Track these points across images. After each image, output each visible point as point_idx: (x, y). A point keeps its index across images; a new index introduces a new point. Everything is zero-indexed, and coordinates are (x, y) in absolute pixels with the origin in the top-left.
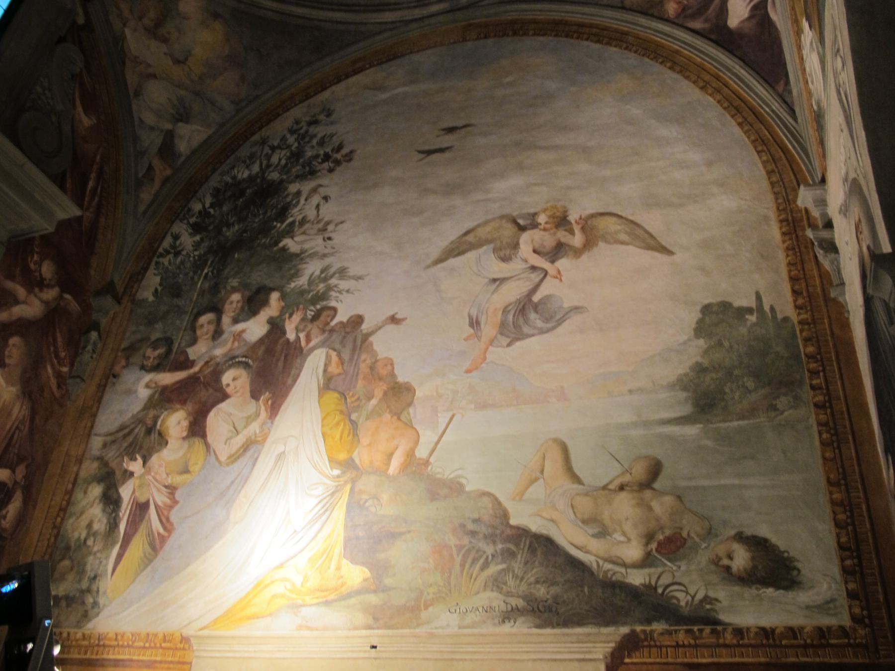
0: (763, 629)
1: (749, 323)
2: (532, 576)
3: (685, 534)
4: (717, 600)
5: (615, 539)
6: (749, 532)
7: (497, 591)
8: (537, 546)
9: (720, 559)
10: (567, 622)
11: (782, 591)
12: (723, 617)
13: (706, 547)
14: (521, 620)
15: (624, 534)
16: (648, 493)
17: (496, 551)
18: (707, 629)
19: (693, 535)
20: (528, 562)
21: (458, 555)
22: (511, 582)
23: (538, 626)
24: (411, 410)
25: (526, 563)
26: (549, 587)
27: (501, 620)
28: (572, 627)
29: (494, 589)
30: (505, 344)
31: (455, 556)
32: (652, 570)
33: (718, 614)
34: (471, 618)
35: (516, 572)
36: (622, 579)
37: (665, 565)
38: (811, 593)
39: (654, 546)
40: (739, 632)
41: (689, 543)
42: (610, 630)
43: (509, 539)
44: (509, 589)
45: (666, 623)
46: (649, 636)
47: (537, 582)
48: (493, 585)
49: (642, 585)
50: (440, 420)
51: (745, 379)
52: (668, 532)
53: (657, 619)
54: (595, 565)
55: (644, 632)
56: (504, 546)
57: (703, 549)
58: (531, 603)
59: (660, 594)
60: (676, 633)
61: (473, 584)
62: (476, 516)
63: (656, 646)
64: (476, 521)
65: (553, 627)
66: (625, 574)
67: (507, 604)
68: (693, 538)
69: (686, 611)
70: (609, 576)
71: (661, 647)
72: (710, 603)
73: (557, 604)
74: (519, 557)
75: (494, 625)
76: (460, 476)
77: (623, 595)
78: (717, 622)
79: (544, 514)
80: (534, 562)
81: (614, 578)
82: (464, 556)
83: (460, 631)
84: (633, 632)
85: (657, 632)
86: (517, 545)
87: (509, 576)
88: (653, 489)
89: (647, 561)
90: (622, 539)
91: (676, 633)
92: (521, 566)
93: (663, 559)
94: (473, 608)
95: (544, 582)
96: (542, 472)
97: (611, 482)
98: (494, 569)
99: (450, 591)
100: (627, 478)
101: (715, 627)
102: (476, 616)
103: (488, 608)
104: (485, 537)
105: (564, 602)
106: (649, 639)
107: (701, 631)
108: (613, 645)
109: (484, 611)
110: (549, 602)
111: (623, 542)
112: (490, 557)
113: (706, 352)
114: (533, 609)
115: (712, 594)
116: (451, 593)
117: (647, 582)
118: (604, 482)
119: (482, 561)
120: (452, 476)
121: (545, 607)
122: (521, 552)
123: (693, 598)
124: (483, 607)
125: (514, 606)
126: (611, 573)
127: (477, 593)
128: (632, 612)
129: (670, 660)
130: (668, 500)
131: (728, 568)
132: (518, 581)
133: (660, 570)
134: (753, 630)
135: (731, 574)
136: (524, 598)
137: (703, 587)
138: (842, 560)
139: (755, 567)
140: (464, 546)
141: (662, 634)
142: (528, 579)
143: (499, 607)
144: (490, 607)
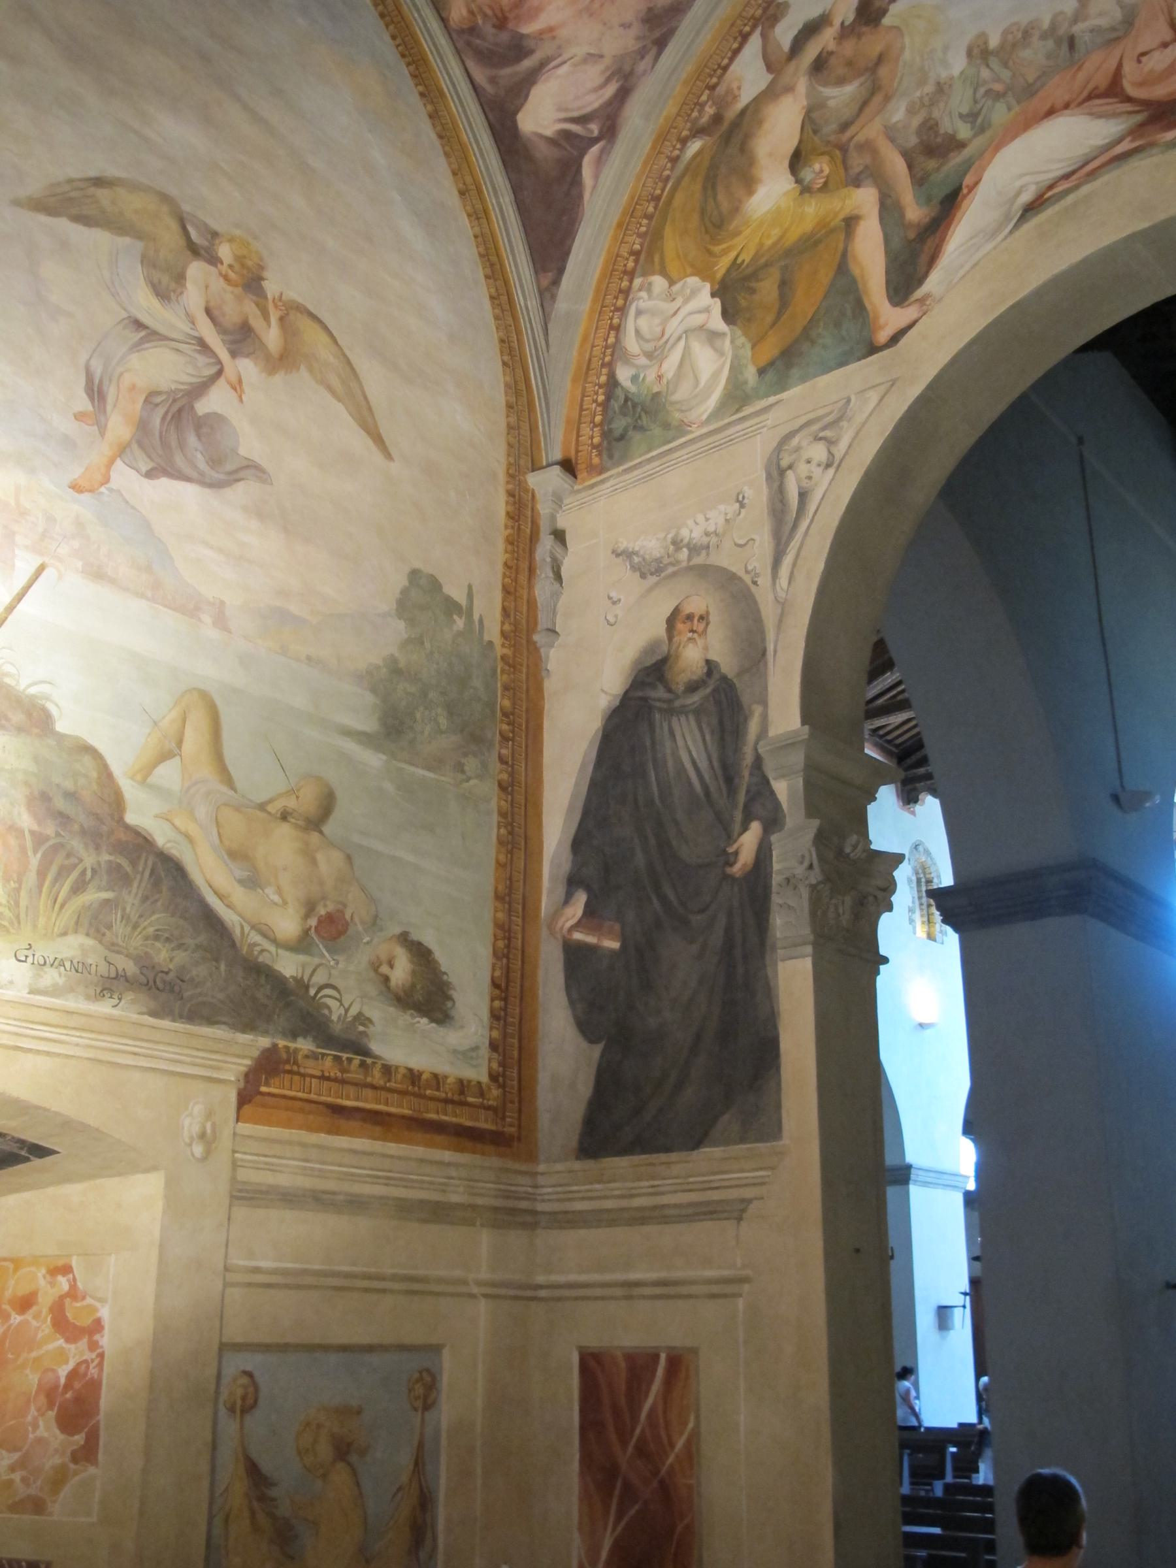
0: (410, 1070)
1: (455, 628)
2: (150, 925)
3: (348, 917)
5: (267, 896)
6: (415, 936)
7: (95, 938)
9: (381, 964)
10: (192, 1016)
11: (434, 1025)
12: (375, 1047)
13: (368, 943)
14: (129, 996)
15: (279, 892)
16: (314, 837)
17: (99, 863)
18: (357, 1059)
19: (356, 919)
21: (35, 852)
22: (120, 928)
23: (154, 1014)
25: (145, 899)
26: (173, 950)
27: (98, 992)
28: (200, 1025)
31: (30, 853)
33: (369, 1041)
34: (52, 976)
35: (128, 910)
36: (269, 962)
37: (323, 956)
39: (313, 922)
40: (387, 1070)
41: (351, 931)
43: (119, 848)
45: (314, 1041)
46: (292, 1055)
47: (157, 938)
48: (90, 924)
49: (292, 977)
52: (331, 907)
53: (305, 1033)
54: (238, 932)
55: (287, 1048)
56: (112, 858)
57: (365, 943)
58: (145, 971)
59: (311, 997)
60: (322, 1059)
62: (69, 785)
64: (71, 796)
65: (174, 1020)
66: (274, 953)
67: (110, 963)
68: (356, 924)
69: (337, 1028)
70: (256, 953)
71: (303, 1076)
72: (363, 1025)
73: (183, 981)
74: (135, 885)
75: (88, 998)
76: (47, 698)
77: (269, 987)
78: (365, 1052)
79: (177, 822)
80: (156, 901)
81: (260, 959)
82: (44, 855)
83: (32, 996)
84: (275, 1046)
85: (301, 1053)
86: (134, 863)
87: (116, 914)
88: (321, 832)
89: (301, 945)
90: (276, 898)
91: (322, 1059)
92: (137, 902)
93: (321, 946)
94: (56, 958)
95: (168, 940)
96: (180, 743)
97: (270, 801)
98: (93, 896)
99: (18, 917)
100: (291, 803)
101: (365, 1059)
102: (60, 975)
103: (80, 965)
104: (83, 832)
105: (192, 980)
106: (292, 1061)
107: (350, 1060)
108: (248, 1062)
109: (73, 969)
111: (275, 904)
112: (89, 873)
113: (406, 644)
114: (148, 982)
115: (368, 1013)
116: (19, 923)
117: (299, 976)
118: (263, 797)
119: (75, 875)
120: (32, 691)
121: (164, 982)
122: (138, 876)
123: (347, 1011)
124: (72, 962)
125: (120, 970)
126: (258, 948)
127: (64, 934)
128: (276, 1016)
129: (313, 1096)
130: (337, 856)
131: (387, 979)
132: (129, 929)
133: (316, 960)
135: (388, 988)
136: (137, 959)
137: (358, 1000)
138: (492, 1000)
139: (413, 986)
140: (47, 839)
141: (307, 1057)
142: (145, 928)
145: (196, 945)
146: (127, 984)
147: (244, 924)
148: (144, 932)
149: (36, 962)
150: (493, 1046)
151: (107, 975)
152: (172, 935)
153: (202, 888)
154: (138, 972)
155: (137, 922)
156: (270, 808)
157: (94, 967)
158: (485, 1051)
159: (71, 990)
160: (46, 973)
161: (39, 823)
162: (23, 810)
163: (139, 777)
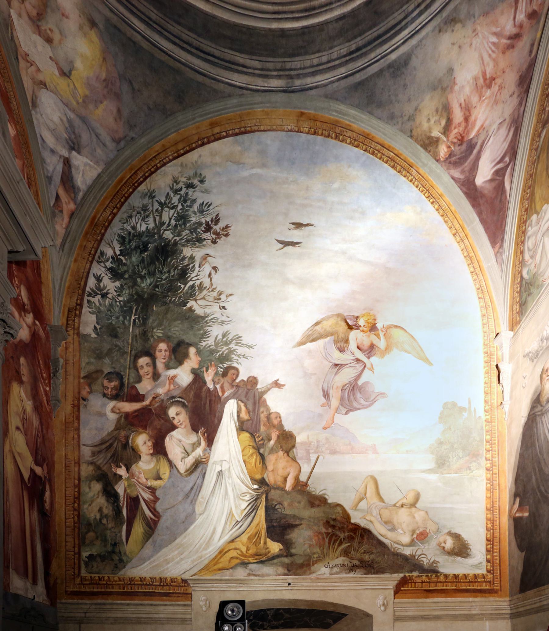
0: (455, 575)
3: (428, 531)
4: (438, 562)
12: (441, 570)
15: (403, 530)
16: (413, 509)
19: (431, 531)
23: (365, 574)
24: (294, 450)
30: (344, 412)
32: (414, 548)
38: (473, 559)
39: (415, 536)
41: (429, 536)
42: (396, 575)
50: (311, 458)
51: (459, 451)
52: (421, 530)
63: (414, 582)
69: (426, 567)
78: (438, 572)
84: (405, 576)
86: (355, 534)
88: (416, 507)
90: (402, 532)
96: (365, 494)
98: (344, 546)
100: (404, 501)
105: (376, 562)
107: (431, 575)
115: (437, 559)
118: (394, 502)
119: (338, 541)
127: (337, 558)
130: (422, 513)
133: (417, 548)
134: (451, 575)
138: (487, 546)
140: (330, 533)
150: (488, 561)
156: (397, 505)
158: (485, 563)
161: (327, 529)
162: (322, 527)
163: (354, 508)
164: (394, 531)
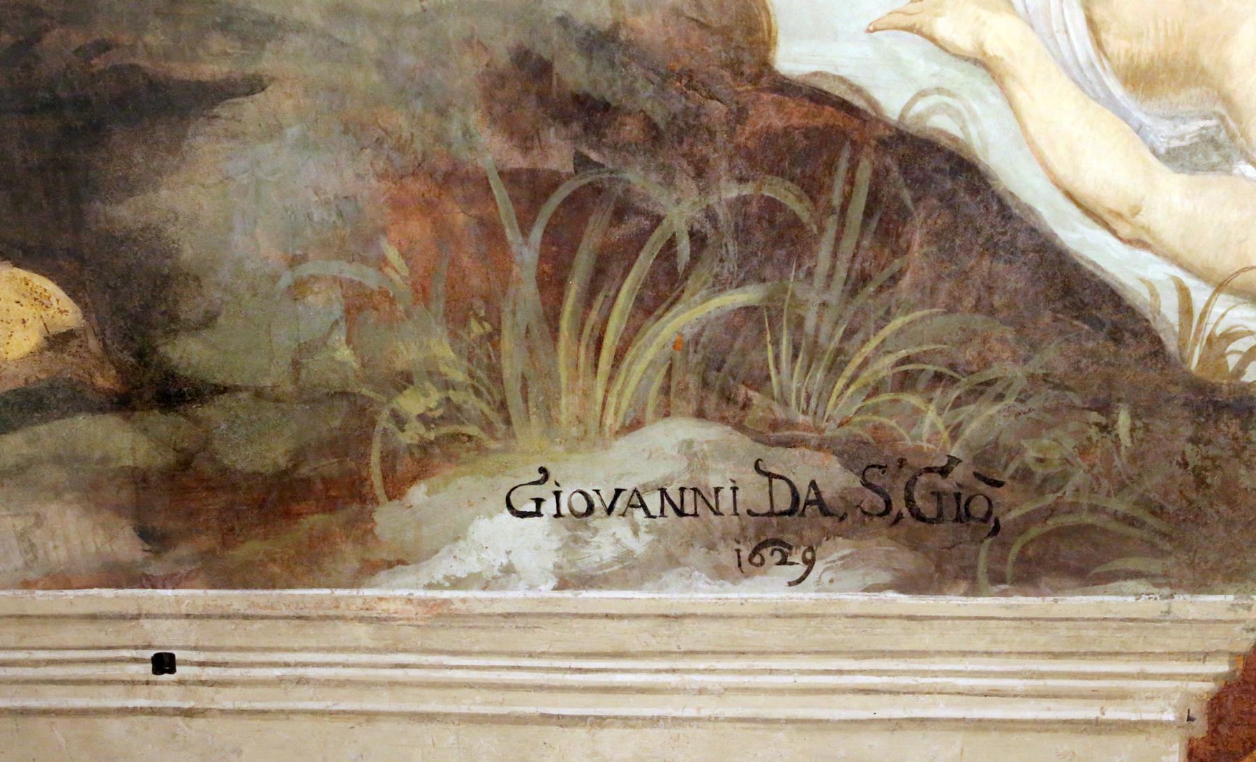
7: (723, 420)
8: (906, 195)
14: (836, 550)
17: (711, 216)
20: (864, 278)
23: (908, 585)
26: (958, 403)
27: (745, 553)
29: (712, 400)
44: (780, 413)
48: (705, 384)
54: (1169, 309)
61: (611, 379)
67: (771, 476)
75: (719, 573)
80: (894, 279)
87: (776, 343)
92: (835, 295)
94: (618, 492)
103: (689, 496)
105: (1025, 475)
109: (669, 510)
110: (959, 473)
121: (938, 495)
124: (663, 492)
127: (634, 425)
142: (865, 363)
143: (734, 489)
144: (695, 490)
145: (1032, 377)
146: (828, 522)
147: (1190, 282)
148: (866, 375)
149: (565, 510)
151: (766, 508)
152: (952, 366)
153: (1040, 208)
154: (859, 485)
155: (839, 351)
157: (727, 493)
159: (672, 561)
160: (596, 531)
164: (1223, 166)
